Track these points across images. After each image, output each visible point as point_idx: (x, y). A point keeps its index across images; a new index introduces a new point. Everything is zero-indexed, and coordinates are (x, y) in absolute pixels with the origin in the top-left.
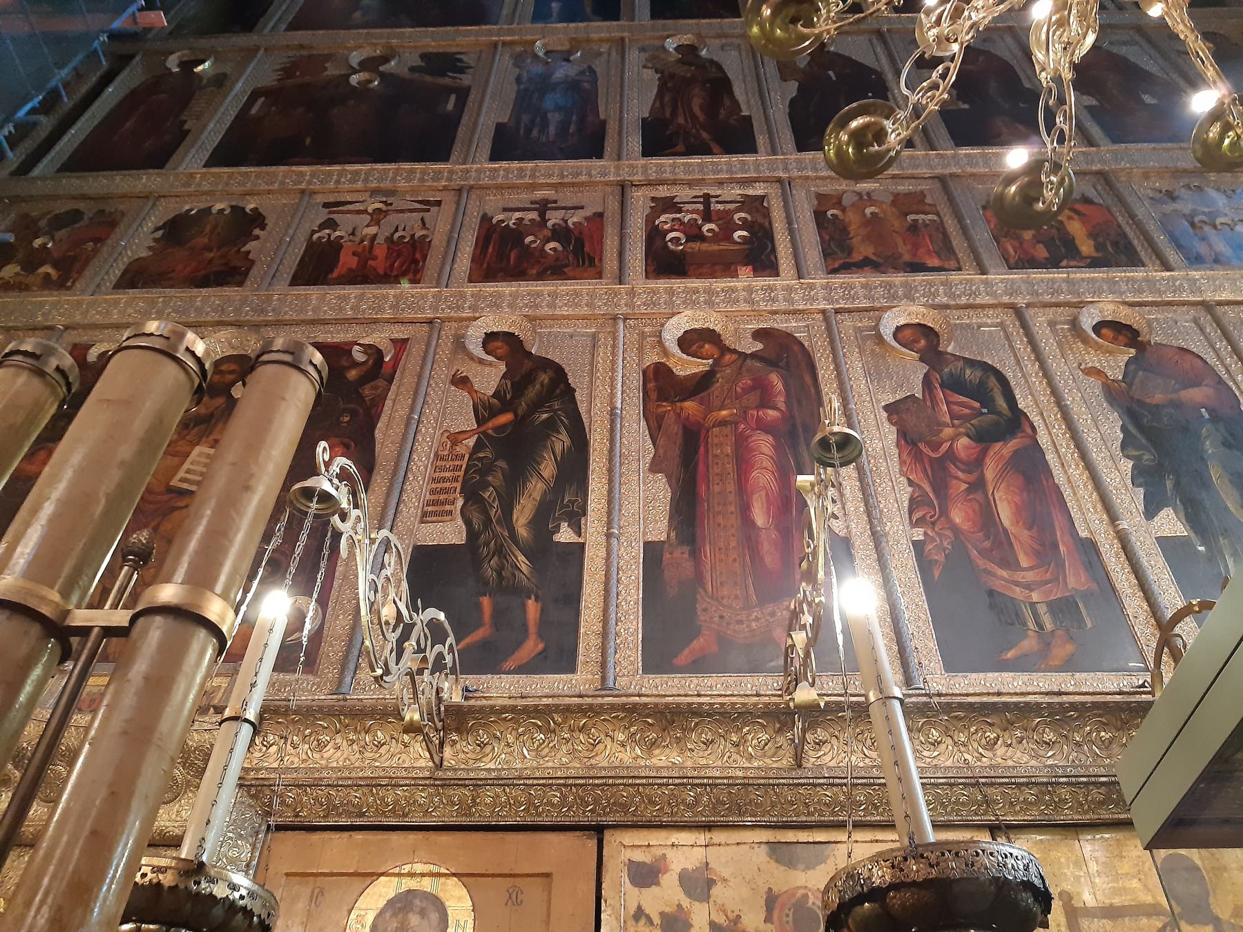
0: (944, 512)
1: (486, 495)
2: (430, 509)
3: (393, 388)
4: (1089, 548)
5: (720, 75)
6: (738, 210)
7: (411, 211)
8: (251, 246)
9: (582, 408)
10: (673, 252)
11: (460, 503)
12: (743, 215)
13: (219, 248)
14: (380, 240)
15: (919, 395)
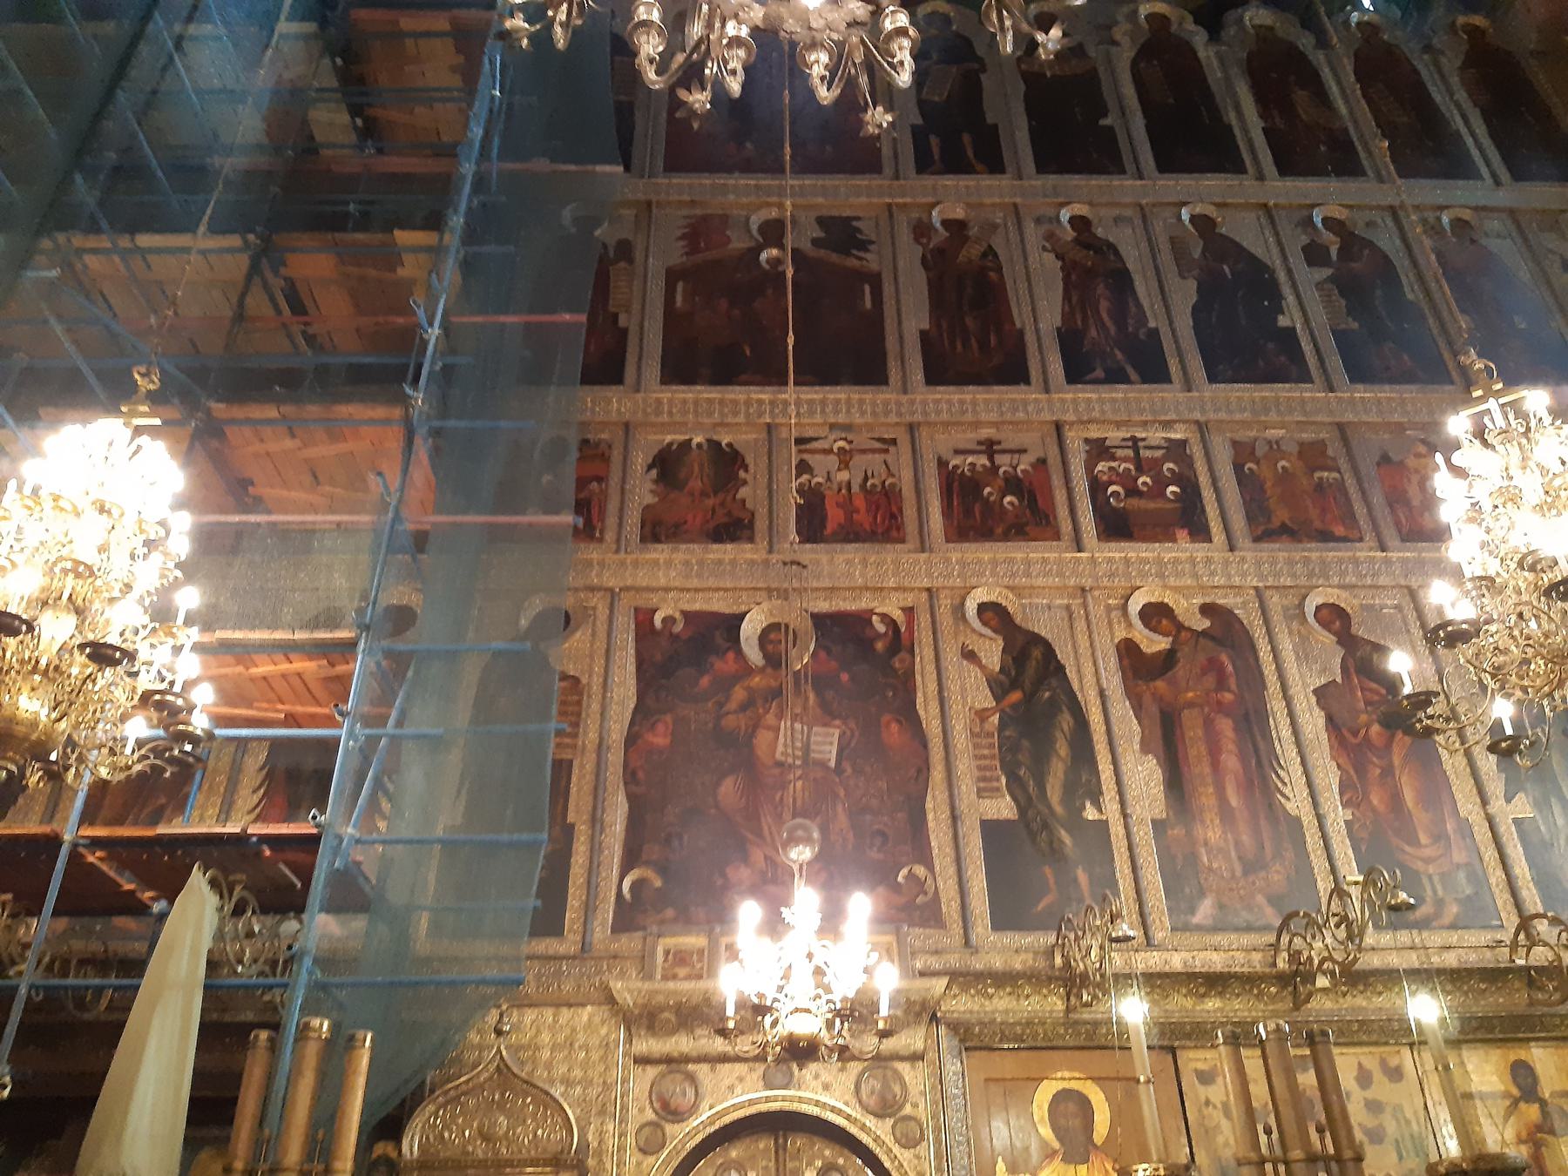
0: (1366, 795)
1: (1022, 773)
2: (982, 785)
3: (918, 659)
4: (1465, 828)
5: (1119, 265)
6: (1165, 459)
7: (874, 451)
8: (743, 492)
9: (1076, 686)
10: (1114, 509)
11: (1004, 780)
12: (1171, 465)
13: (715, 493)
14: (855, 488)
15: (1339, 680)
